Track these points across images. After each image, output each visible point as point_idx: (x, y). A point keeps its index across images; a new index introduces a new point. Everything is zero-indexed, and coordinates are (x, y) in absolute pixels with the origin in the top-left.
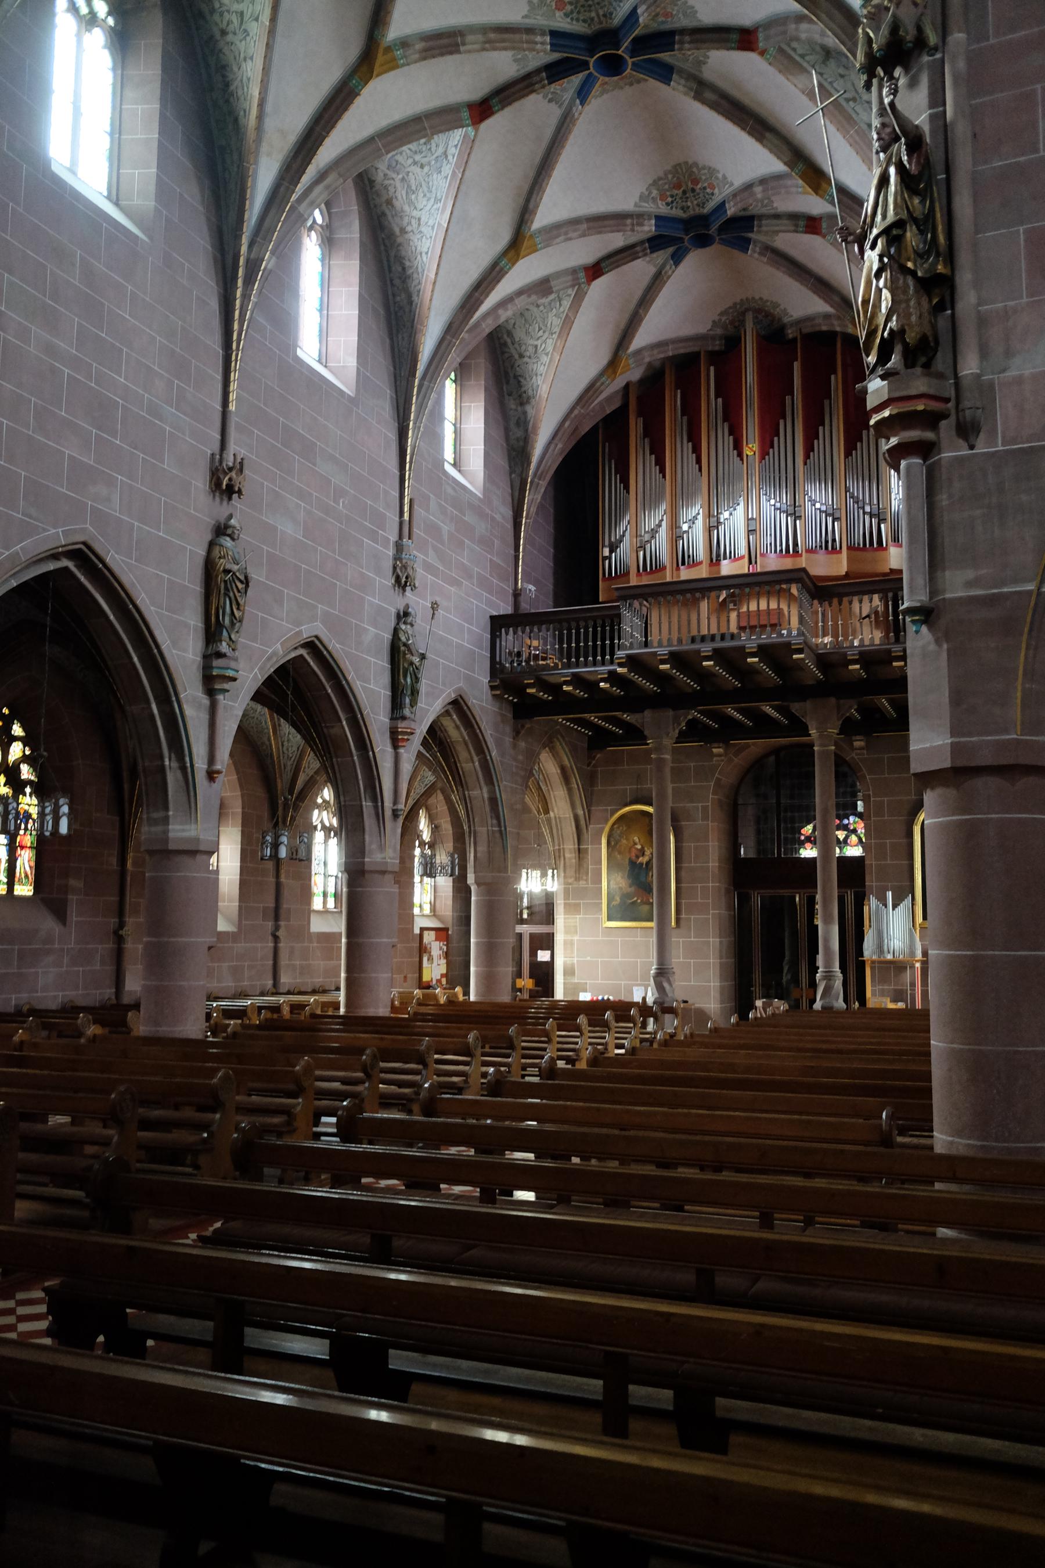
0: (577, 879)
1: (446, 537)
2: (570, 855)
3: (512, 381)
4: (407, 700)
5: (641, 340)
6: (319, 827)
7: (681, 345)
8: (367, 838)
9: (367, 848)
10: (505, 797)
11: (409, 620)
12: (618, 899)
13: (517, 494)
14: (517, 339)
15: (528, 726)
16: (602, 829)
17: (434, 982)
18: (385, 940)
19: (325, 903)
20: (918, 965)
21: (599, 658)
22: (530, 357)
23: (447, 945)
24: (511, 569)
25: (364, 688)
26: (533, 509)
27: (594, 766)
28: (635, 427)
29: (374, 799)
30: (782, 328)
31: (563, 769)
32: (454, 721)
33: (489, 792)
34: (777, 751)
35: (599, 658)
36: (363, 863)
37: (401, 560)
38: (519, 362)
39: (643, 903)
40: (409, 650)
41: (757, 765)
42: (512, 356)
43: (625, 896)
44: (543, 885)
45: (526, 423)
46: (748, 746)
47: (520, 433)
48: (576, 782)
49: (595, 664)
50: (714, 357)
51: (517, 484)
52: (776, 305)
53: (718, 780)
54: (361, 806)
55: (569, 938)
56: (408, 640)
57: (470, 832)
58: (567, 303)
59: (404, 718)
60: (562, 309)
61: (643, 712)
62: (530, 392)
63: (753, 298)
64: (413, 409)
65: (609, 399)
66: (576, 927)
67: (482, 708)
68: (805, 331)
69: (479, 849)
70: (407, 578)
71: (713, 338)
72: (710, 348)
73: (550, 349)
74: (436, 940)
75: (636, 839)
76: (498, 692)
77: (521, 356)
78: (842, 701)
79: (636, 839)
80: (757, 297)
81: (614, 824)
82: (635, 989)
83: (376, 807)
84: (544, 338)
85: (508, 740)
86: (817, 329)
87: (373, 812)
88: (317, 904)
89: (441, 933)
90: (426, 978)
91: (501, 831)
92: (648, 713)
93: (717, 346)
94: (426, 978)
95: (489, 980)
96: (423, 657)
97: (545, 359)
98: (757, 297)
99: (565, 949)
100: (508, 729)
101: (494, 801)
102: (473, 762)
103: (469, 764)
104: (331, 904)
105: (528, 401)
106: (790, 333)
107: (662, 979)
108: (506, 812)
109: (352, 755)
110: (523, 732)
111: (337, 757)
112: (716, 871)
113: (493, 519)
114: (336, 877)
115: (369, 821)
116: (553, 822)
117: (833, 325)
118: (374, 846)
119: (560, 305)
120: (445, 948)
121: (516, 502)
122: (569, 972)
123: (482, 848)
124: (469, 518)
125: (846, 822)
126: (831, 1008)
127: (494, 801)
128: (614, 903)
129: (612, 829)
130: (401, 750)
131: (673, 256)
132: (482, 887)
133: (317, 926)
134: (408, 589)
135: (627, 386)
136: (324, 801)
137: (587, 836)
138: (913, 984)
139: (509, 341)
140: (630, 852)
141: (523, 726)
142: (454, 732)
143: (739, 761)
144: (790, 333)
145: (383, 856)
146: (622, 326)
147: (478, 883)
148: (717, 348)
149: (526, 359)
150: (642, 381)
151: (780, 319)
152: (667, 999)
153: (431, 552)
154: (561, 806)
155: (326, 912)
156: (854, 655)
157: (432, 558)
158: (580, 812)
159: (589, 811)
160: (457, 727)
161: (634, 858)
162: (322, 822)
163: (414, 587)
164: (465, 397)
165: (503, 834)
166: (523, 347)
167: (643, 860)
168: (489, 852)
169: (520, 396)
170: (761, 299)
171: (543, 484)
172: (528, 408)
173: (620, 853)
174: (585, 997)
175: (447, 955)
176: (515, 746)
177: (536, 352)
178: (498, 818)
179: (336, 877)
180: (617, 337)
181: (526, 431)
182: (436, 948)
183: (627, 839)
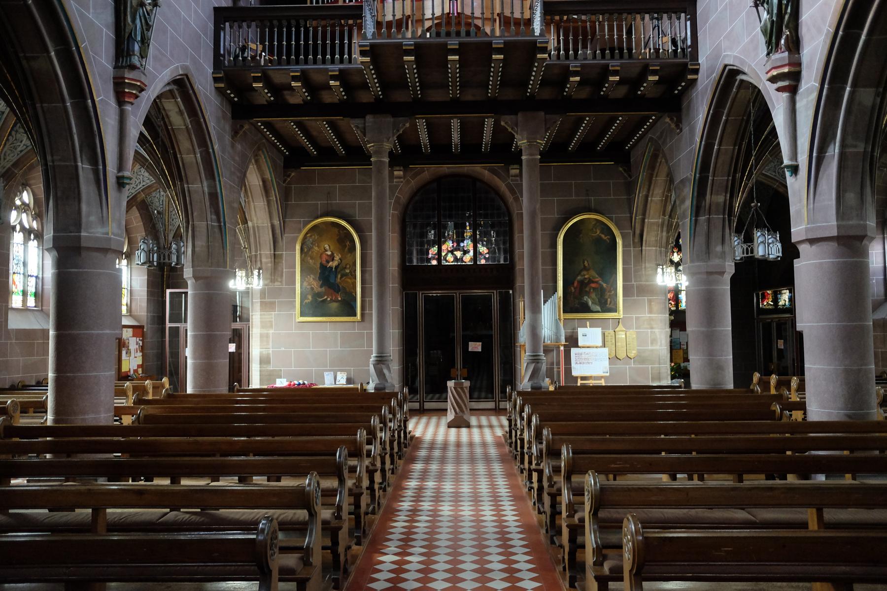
4: (137, 47)
6: (18, 228)
8: (84, 207)
9: (84, 220)
10: (225, 194)
12: (310, 297)
15: (246, 127)
17: (132, 372)
18: (108, 332)
19: (24, 301)
20: (562, 348)
21: (328, 56)
23: (142, 341)
25: (82, 15)
27: (289, 183)
29: (93, 161)
31: (264, 181)
32: (177, 103)
33: (209, 187)
34: (439, 180)
35: (328, 56)
36: (79, 237)
39: (332, 301)
41: (423, 189)
43: (317, 295)
44: (247, 283)
48: (274, 195)
49: (324, 61)
53: (398, 198)
54: (76, 167)
57: (187, 228)
59: (133, 67)
61: (364, 117)
66: (271, 322)
67: (205, 94)
69: (198, 243)
74: (133, 336)
76: (222, 85)
78: (548, 116)
81: (307, 233)
82: (326, 374)
83: (96, 172)
85: (228, 138)
87: (91, 176)
88: (16, 301)
89: (138, 330)
90: (124, 368)
91: (220, 226)
92: (369, 118)
94: (124, 368)
95: (206, 372)
99: (261, 341)
100: (228, 128)
101: (214, 197)
102: (195, 153)
104: (31, 302)
108: (226, 209)
109: (63, 101)
110: (241, 133)
111: (42, 102)
112: (396, 274)
114: (37, 277)
115: (87, 187)
118: (92, 218)
120: (141, 343)
122: (264, 361)
123: (201, 243)
125: (462, 245)
126: (540, 388)
127: (214, 197)
128: (307, 301)
130: (128, 108)
132: (199, 282)
133: (15, 323)
136: (24, 203)
137: (282, 243)
138: (558, 364)
140: (321, 257)
141: (242, 127)
142: (177, 118)
143: (414, 183)
145: (104, 230)
147: (196, 277)
152: (387, 385)
154: (260, 215)
155: (25, 310)
156: (576, 67)
158: (276, 222)
159: (284, 222)
160: (181, 113)
162: (21, 223)
165: (221, 229)
167: (333, 264)
168: (208, 247)
173: (312, 258)
174: (281, 383)
175: (142, 349)
176: (233, 146)
178: (217, 213)
179: (37, 277)
182: (134, 343)
183: (318, 247)
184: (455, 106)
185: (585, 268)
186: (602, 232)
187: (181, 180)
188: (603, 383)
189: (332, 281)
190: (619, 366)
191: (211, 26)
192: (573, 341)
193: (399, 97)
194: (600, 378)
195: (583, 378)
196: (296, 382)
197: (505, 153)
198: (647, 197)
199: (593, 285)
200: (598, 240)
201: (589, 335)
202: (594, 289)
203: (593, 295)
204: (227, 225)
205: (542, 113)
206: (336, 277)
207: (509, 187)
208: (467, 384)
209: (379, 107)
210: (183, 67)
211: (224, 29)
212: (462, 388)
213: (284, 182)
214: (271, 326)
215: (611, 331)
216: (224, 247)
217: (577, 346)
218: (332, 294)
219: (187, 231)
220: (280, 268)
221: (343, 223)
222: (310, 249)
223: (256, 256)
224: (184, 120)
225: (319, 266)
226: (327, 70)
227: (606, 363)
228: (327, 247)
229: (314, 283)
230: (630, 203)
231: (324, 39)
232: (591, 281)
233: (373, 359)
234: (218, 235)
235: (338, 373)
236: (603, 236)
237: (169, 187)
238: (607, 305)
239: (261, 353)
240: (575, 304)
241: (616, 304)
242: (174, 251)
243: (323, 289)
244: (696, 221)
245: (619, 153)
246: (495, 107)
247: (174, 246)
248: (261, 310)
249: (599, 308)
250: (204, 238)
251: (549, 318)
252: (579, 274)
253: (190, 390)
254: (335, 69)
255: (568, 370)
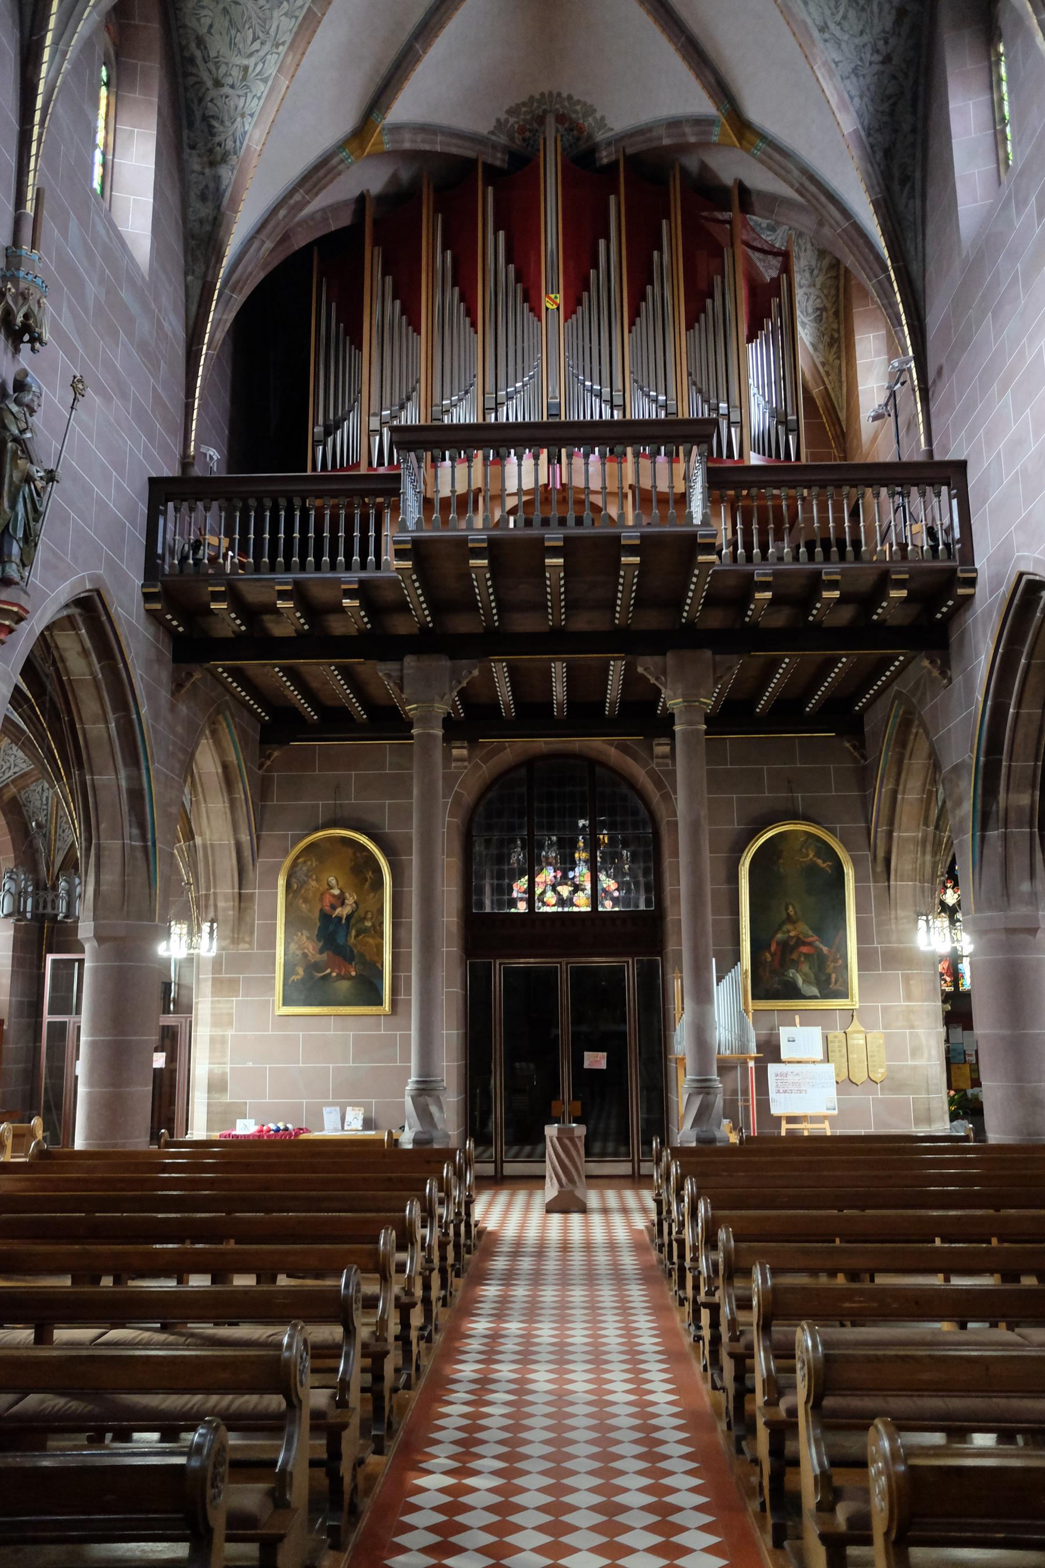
0: (236, 941)
1: (91, 304)
2: (225, 905)
3: (198, 123)
4: (15, 549)
5: (402, 110)
7: (455, 141)
10: (156, 790)
11: (27, 398)
13: (194, 309)
14: (213, 54)
15: (197, 676)
16: (282, 862)
20: (751, 1064)
22: (232, 87)
24: (180, 419)
26: (220, 336)
28: (372, 259)
30: (592, 151)
31: (225, 767)
33: (129, 778)
34: (530, 763)
37: (15, 280)
38: (213, 93)
39: (340, 977)
40: (26, 451)
41: (502, 779)
42: (201, 83)
44: (190, 947)
45: (218, 194)
46: (501, 749)
47: (205, 211)
50: (492, 174)
51: (196, 292)
52: (590, 110)
55: (219, 1032)
56: (22, 432)
61: (400, 659)
62: (230, 144)
63: (559, 95)
64: (52, 24)
65: (335, 209)
66: (230, 1015)
67: (129, 623)
68: (630, 151)
69: (105, 877)
70: (26, 316)
71: (494, 146)
72: (490, 161)
73: (271, 70)
75: (332, 880)
76: (158, 606)
77: (218, 84)
78: (718, 657)
79: (332, 880)
80: (565, 95)
81: (298, 857)
82: (326, 1110)
84: (262, 53)
85: (164, 694)
86: (655, 144)
91: (145, 849)
92: (409, 661)
93: (499, 160)
95: (111, 1109)
96: (51, 477)
97: (261, 88)
98: (565, 95)
99: (212, 1050)
100: (165, 676)
101: (137, 797)
102: (106, 722)
103: (97, 725)
105: (224, 159)
106: (605, 157)
107: (429, 1100)
108: (156, 816)
110: (188, 685)
112: (454, 929)
113: (160, 326)
116: (200, 854)
117: (684, 134)
121: (190, 331)
122: (216, 1086)
123: (111, 877)
124: (125, 295)
125: (571, 875)
126: (712, 1140)
127: (137, 797)
128: (295, 978)
129: (294, 864)
132: (106, 946)
134: (25, 348)
135: (361, 200)
137: (255, 875)
138: (745, 1092)
139: (198, 54)
140: (321, 899)
141: (190, 675)
142: (78, 661)
143: (486, 770)
144: (605, 157)
146: (383, 71)
147: (100, 938)
148: (498, 163)
149: (226, 90)
150: (381, 199)
151: (590, 137)
152: (436, 1134)
153: (65, 309)
154: (216, 825)
156: (765, 575)
157: (66, 324)
158: (245, 838)
159: (258, 837)
160: (85, 653)
161: (327, 908)
163: (36, 339)
164: (123, 116)
166: (223, 70)
167: (343, 912)
169: (211, 151)
170: (570, 97)
171: (239, 299)
172: (226, 174)
173: (306, 900)
174: (246, 1127)
176: (173, 709)
177: (244, 78)
178: (142, 826)
180: (372, 89)
181: (218, 207)
183: (317, 880)
184: (557, 641)
185: (789, 919)
186: (818, 855)
187: (80, 766)
188: (827, 1129)
189: (341, 941)
190: (855, 1096)
191: (143, 508)
192: (770, 1051)
193: (462, 624)
194: (820, 1119)
195: (791, 1120)
196: (272, 1126)
197: (644, 717)
198: (895, 793)
199: (804, 949)
200: (812, 870)
201: (800, 1040)
202: (806, 955)
203: (805, 968)
204: (158, 845)
205: (708, 653)
206: (348, 933)
207: (651, 774)
208: (580, 1130)
209: (426, 643)
210: (92, 578)
211: (165, 513)
212: (572, 1140)
213: (261, 767)
214: (230, 1023)
215: (839, 1033)
216: (150, 883)
217: (778, 1059)
218: (341, 965)
219: (88, 856)
220: (248, 919)
221: (363, 839)
222: (302, 884)
223: (207, 896)
224: (90, 665)
225: (317, 914)
226: (338, 581)
227: (833, 1090)
228: (334, 881)
229: (309, 945)
230: (866, 803)
231: (334, 530)
232: (800, 942)
233: (410, 1087)
234: (141, 863)
235: (349, 1109)
236: (820, 862)
237: (59, 779)
238: (830, 985)
239: (211, 1073)
240: (772, 983)
241: (846, 983)
242: (62, 893)
243: (325, 956)
244: (983, 839)
245: (844, 717)
246: (627, 642)
247: (63, 884)
248: (214, 993)
249: (815, 991)
250: (118, 868)
251: (723, 1010)
252: (779, 929)
253: (79, 1143)
254: (351, 578)
255: (764, 1104)
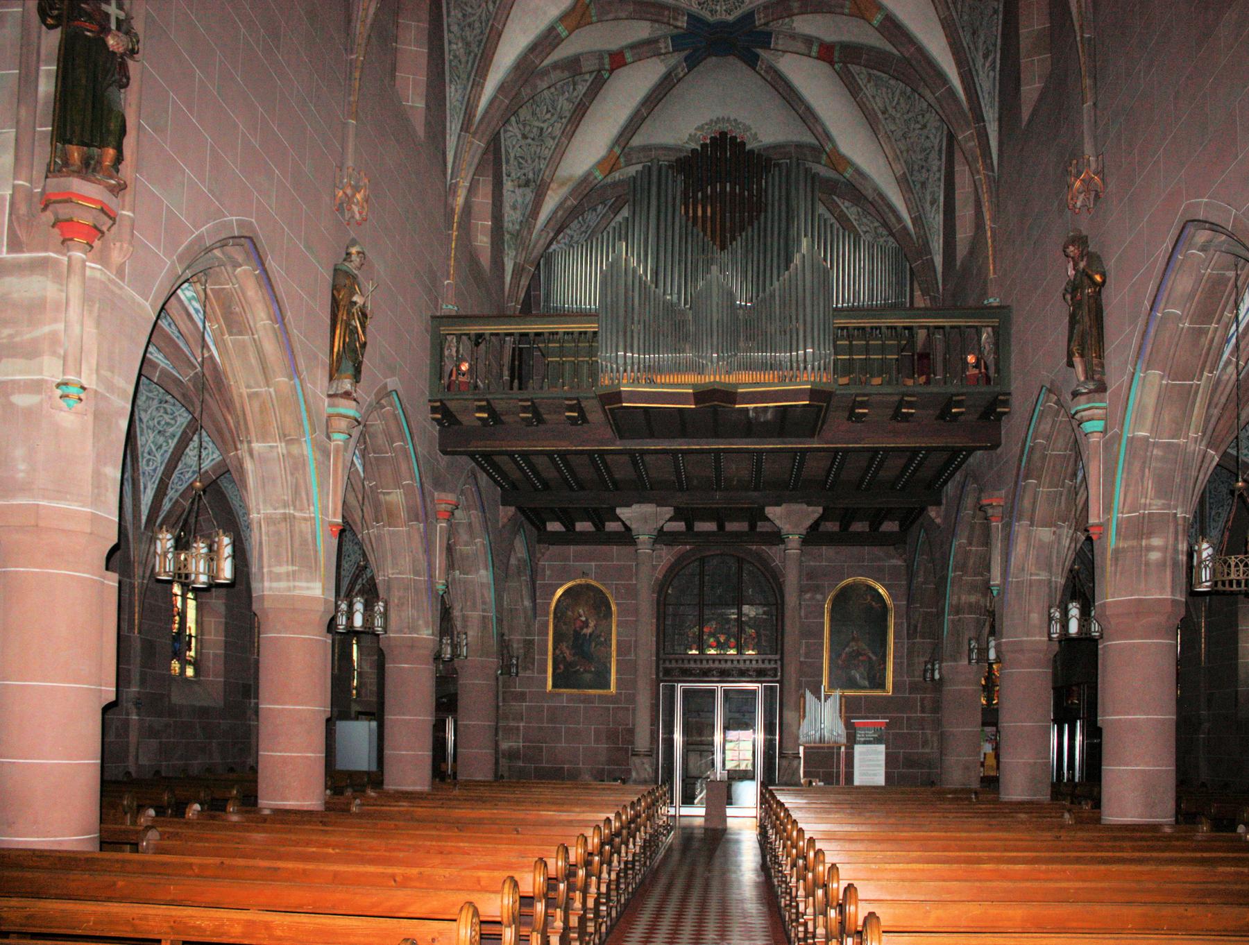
58: (582, 89)
60: (575, 94)
73: (558, 133)
75: (581, 611)
119: (574, 89)
131: (686, 59)
167: (587, 631)
243: (576, 658)
